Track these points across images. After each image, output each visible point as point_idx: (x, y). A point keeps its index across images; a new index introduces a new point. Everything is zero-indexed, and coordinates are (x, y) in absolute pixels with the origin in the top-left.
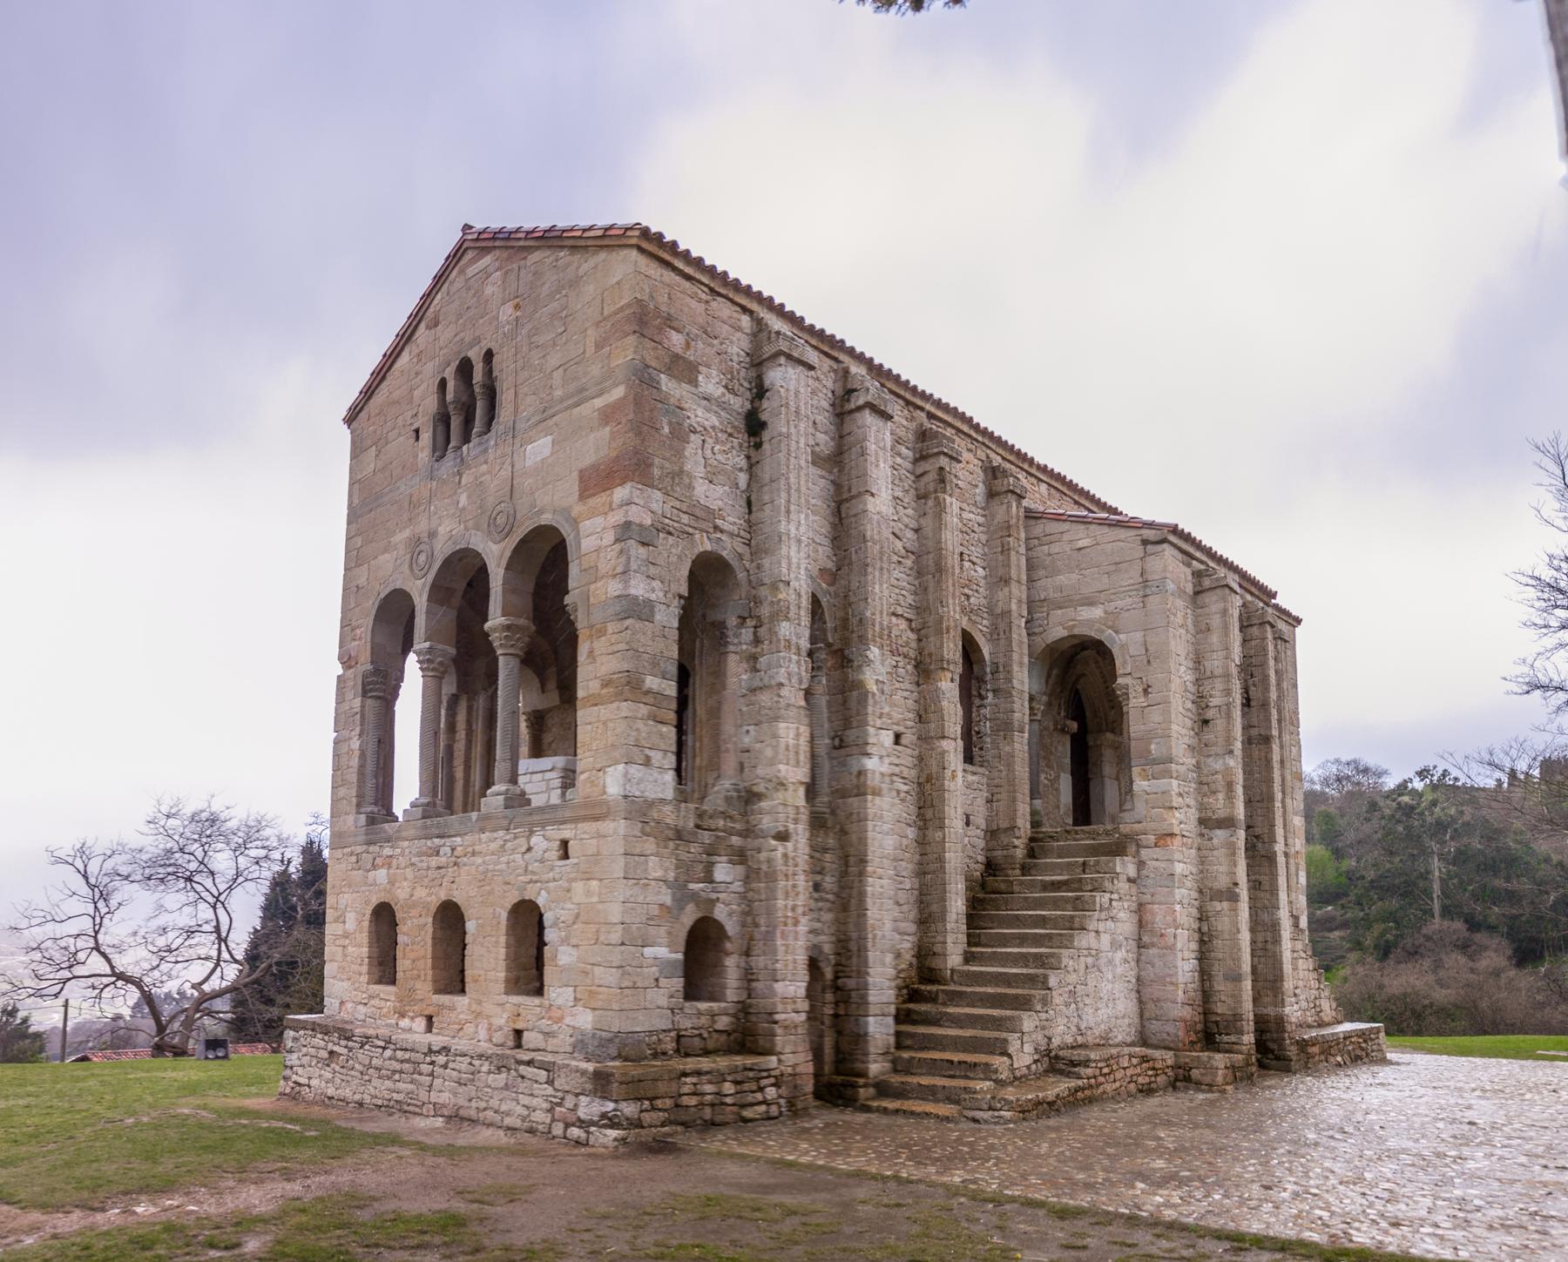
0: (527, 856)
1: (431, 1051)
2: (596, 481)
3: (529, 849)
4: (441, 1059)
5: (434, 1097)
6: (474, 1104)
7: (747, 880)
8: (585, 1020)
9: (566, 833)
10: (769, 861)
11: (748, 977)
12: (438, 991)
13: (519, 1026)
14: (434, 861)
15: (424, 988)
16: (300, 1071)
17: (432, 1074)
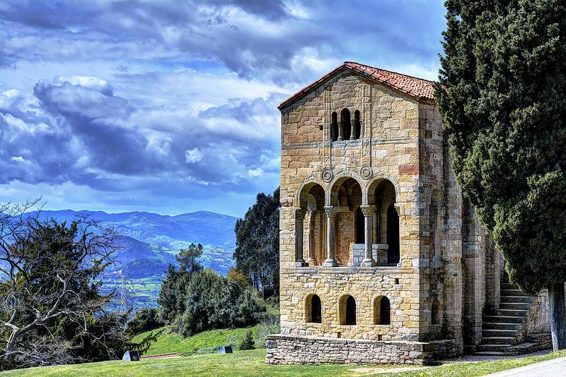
0: (382, 283)
1: (347, 343)
2: (404, 170)
3: (383, 280)
4: (353, 345)
5: (349, 357)
6: (368, 358)
7: (445, 287)
8: (406, 331)
9: (398, 277)
10: (452, 282)
11: (445, 316)
12: (342, 324)
13: (380, 333)
14: (339, 282)
15: (336, 324)
16: (278, 354)
17: (348, 350)
